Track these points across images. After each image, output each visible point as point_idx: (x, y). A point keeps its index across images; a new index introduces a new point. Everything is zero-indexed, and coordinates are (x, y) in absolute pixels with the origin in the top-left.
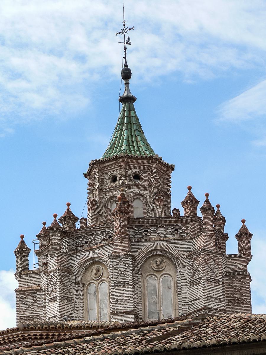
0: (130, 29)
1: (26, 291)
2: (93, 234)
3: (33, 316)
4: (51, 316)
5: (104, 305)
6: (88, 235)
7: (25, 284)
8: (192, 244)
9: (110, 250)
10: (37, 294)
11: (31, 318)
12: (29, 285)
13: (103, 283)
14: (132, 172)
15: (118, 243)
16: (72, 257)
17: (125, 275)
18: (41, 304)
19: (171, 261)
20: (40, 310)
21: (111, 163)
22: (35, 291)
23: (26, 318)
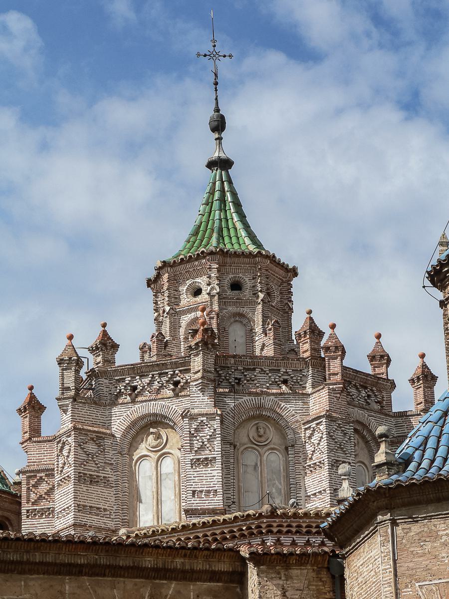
0: (225, 56)
1: (90, 431)
2: (254, 369)
3: (98, 476)
4: (201, 489)
5: (274, 490)
6: (244, 369)
7: (82, 418)
8: (395, 425)
9: (297, 404)
10: (105, 441)
11: (95, 478)
12: (88, 422)
13: (273, 454)
14: (229, 278)
15: (333, 396)
16: (220, 398)
17: (344, 451)
18: (110, 459)
19: (366, 442)
20: (108, 469)
21: (241, 260)
22: (103, 436)
23: (88, 477)
